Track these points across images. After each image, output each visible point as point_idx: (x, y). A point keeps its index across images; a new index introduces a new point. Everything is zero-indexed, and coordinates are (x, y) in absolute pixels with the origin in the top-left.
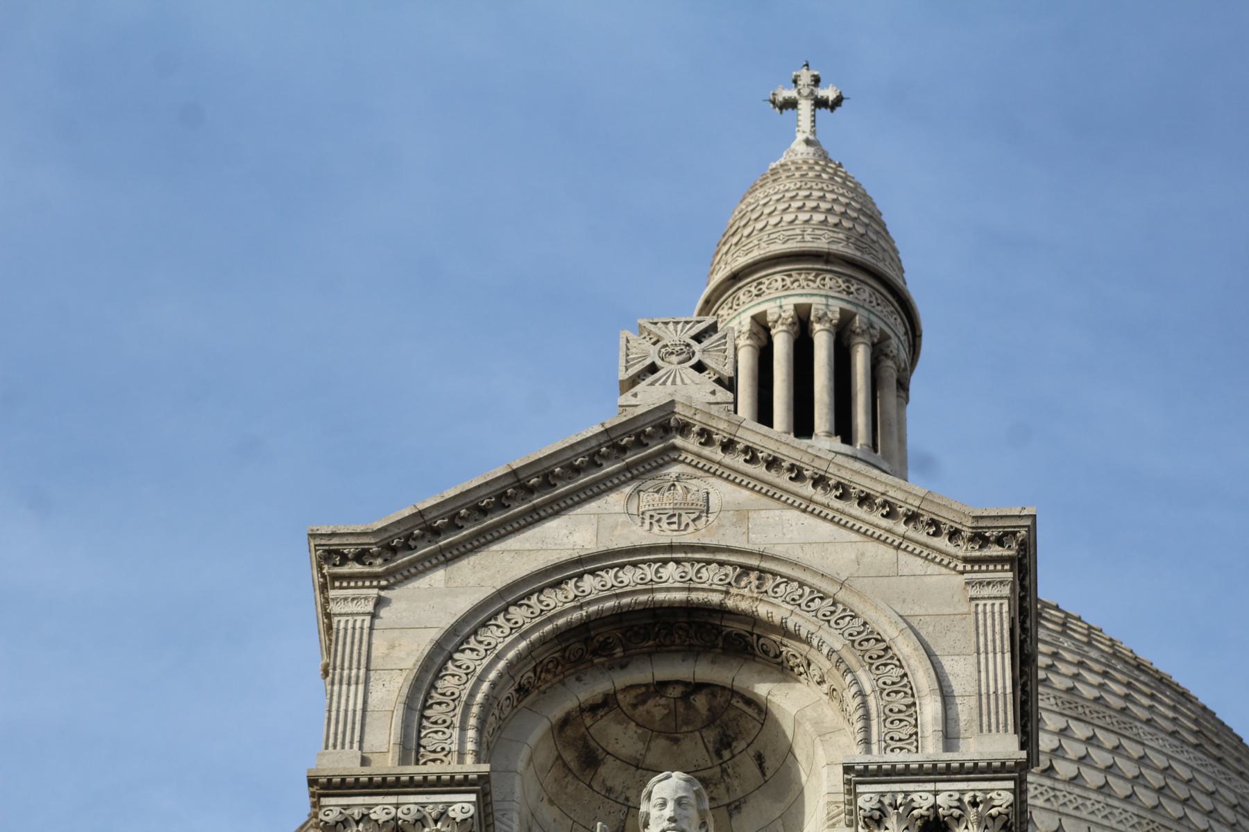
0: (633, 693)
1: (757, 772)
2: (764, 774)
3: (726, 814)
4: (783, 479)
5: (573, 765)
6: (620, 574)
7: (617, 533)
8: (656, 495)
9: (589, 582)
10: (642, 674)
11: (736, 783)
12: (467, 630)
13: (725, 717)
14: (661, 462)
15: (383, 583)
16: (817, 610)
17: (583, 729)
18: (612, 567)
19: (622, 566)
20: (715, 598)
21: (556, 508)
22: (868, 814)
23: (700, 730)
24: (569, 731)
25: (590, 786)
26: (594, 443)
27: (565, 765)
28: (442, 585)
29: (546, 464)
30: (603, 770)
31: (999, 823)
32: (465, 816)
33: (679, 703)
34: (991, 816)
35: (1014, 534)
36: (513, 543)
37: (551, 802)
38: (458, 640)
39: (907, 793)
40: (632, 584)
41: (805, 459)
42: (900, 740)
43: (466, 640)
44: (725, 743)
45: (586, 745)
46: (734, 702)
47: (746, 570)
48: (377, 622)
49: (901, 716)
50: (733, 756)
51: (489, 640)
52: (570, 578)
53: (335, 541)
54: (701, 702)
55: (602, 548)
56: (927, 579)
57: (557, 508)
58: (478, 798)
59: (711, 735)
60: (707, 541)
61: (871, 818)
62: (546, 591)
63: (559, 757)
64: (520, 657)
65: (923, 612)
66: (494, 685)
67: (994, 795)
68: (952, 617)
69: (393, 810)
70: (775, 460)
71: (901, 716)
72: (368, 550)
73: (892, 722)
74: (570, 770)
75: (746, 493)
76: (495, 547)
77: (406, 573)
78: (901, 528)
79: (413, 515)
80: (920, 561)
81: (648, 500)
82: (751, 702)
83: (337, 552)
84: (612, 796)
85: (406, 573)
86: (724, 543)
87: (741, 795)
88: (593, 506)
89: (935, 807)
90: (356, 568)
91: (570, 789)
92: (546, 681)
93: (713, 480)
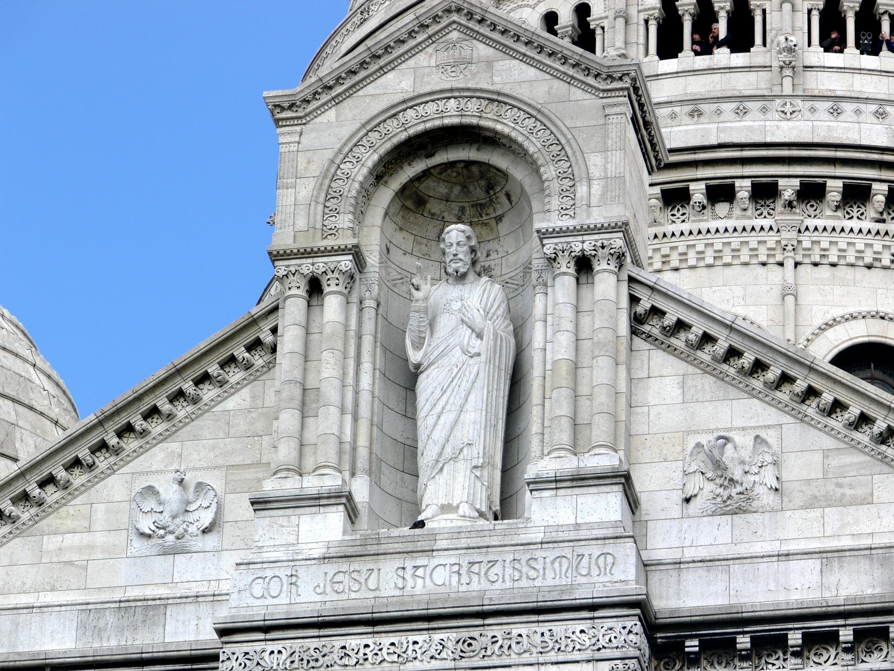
0: (439, 168)
1: (508, 202)
2: (511, 204)
3: (494, 222)
4: (509, 42)
5: (411, 207)
6: (426, 108)
7: (424, 80)
8: (446, 53)
9: (410, 113)
10: (441, 158)
11: (498, 206)
12: (346, 150)
13: (488, 175)
14: (447, 31)
15: (304, 121)
16: (527, 126)
17: (415, 189)
18: (421, 104)
19: (427, 102)
20: (474, 121)
21: (393, 66)
22: (548, 257)
23: (477, 181)
24: (407, 192)
25: (423, 215)
26: (411, 25)
27: (407, 208)
28: (333, 120)
29: (385, 42)
30: (428, 206)
31: (615, 257)
32: (346, 269)
33: (464, 170)
34: (610, 254)
35: (628, 74)
36: (370, 89)
37: (401, 229)
38: (342, 156)
39: (568, 243)
40: (432, 114)
41: (521, 31)
42: (567, 209)
43: (346, 156)
44: (490, 187)
45: (418, 196)
46: (491, 169)
47: (492, 101)
48: (300, 146)
49: (567, 194)
50: (495, 194)
51: (358, 155)
52: (400, 112)
53: (278, 100)
54: (475, 169)
55: (416, 94)
56: (585, 102)
57: (392, 66)
58: (353, 256)
59: (483, 183)
60: (471, 85)
61: (550, 258)
62: (388, 121)
63: (403, 205)
64: (376, 166)
65: (581, 125)
66: (361, 183)
67: (612, 241)
68: (596, 127)
69: (311, 267)
70: (506, 30)
71: (567, 194)
72: (295, 104)
73: (562, 198)
74: (410, 210)
75: (491, 49)
76: (360, 93)
77: (315, 114)
78: (571, 72)
79: (317, 81)
80: (581, 91)
81: (443, 56)
82: (499, 170)
83: (279, 106)
84: (435, 217)
85: (315, 114)
86: (478, 86)
87: (500, 212)
88: (411, 63)
89: (582, 250)
90: (289, 114)
91: (411, 219)
92: (392, 168)
93: (475, 42)
